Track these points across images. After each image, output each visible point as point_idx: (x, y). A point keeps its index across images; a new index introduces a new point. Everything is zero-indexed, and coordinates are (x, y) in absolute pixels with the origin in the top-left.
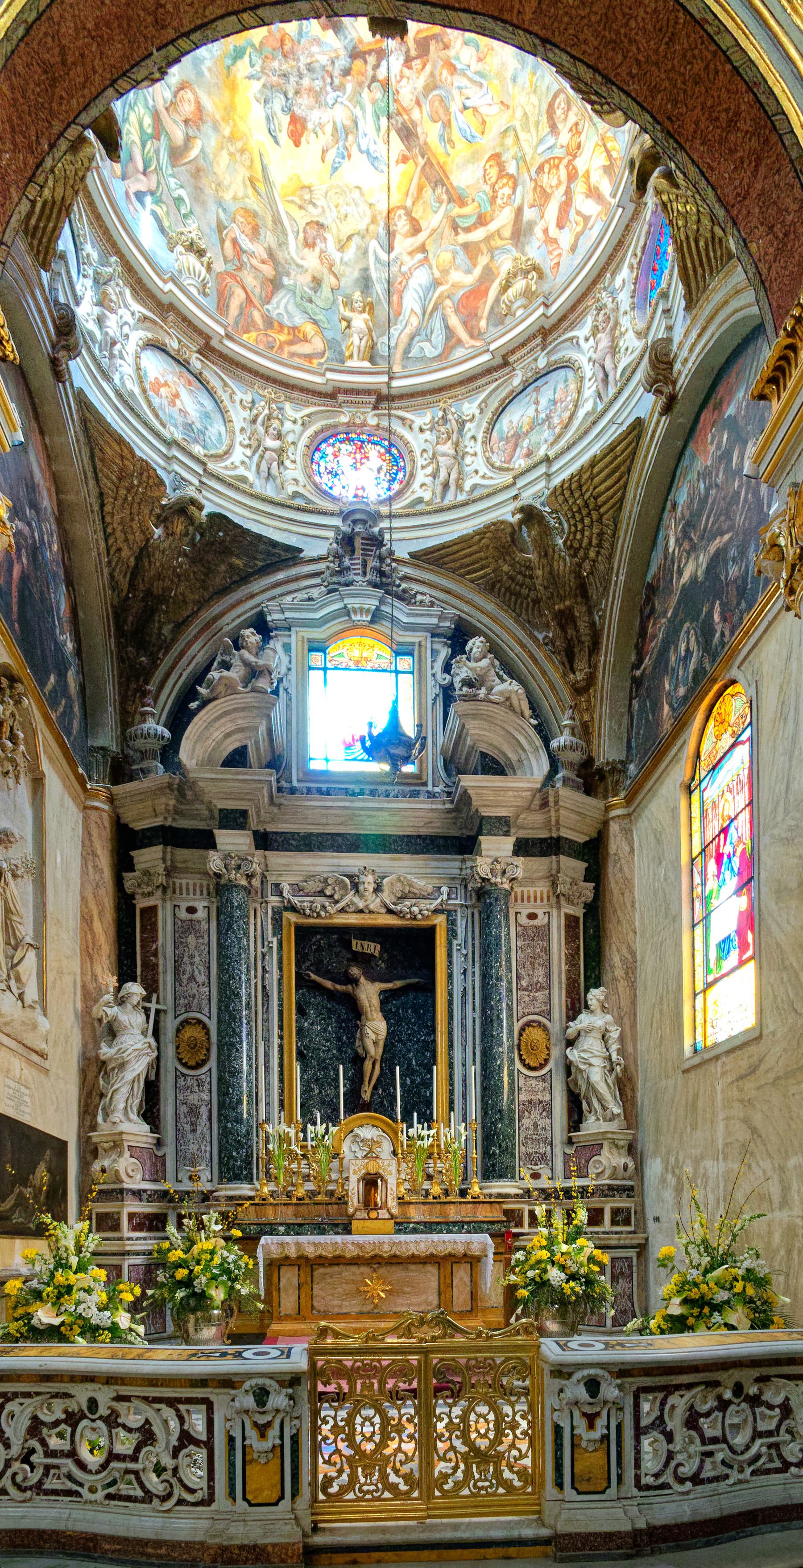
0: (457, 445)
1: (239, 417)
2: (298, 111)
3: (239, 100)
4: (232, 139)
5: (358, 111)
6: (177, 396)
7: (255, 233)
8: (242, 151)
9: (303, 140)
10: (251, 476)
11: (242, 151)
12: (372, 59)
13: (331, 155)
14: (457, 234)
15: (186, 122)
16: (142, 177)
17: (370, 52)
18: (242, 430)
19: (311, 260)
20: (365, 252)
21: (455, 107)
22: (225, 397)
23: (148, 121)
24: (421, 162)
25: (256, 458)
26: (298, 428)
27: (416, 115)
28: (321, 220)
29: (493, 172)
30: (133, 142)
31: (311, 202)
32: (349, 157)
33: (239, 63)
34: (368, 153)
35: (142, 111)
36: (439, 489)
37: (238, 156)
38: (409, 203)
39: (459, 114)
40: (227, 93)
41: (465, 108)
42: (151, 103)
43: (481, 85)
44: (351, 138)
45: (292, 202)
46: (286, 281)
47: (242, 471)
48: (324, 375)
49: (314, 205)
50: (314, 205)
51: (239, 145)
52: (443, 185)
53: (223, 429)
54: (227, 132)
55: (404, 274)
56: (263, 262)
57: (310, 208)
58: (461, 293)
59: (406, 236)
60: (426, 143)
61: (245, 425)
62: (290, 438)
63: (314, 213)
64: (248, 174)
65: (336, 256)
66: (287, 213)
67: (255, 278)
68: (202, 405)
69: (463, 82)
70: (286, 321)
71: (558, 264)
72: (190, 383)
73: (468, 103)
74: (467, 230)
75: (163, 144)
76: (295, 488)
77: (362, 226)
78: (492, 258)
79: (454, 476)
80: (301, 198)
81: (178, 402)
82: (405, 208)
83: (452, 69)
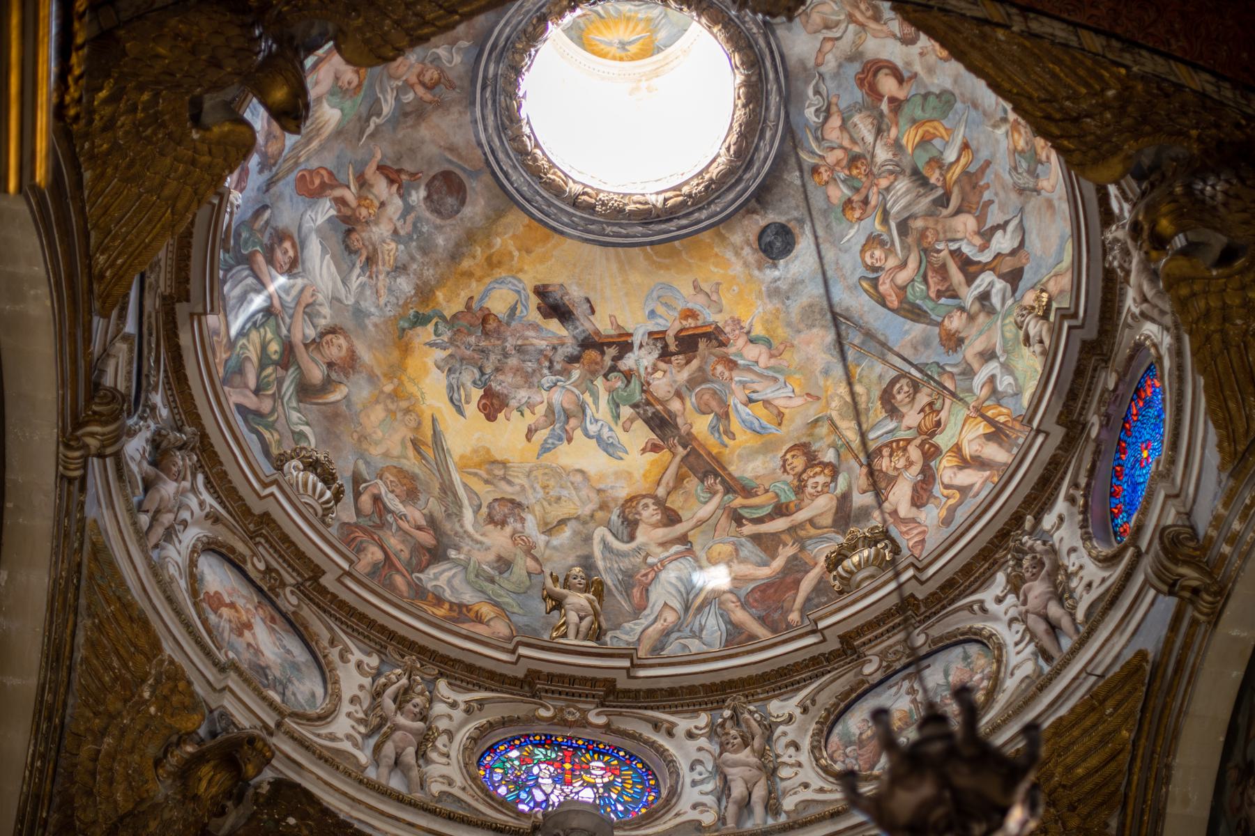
0: (762, 754)
1: (352, 681)
2: (496, 387)
3: (412, 363)
4: (395, 396)
5: (587, 398)
6: (249, 626)
7: (411, 495)
8: (407, 411)
9: (501, 416)
10: (363, 757)
11: (407, 411)
12: (612, 352)
13: (543, 434)
14: (740, 524)
15: (330, 365)
16: (252, 395)
17: (610, 345)
18: (354, 700)
19: (499, 540)
20: (588, 539)
21: (736, 400)
22: (334, 654)
23: (274, 347)
24: (681, 451)
25: (372, 742)
26: (458, 714)
27: (675, 405)
28: (518, 499)
29: (799, 463)
30: (248, 358)
31: (504, 478)
32: (570, 440)
33: (419, 329)
34: (599, 438)
35: (269, 335)
36: (732, 810)
37: (399, 415)
38: (661, 492)
39: (740, 407)
40: (396, 354)
41: (751, 401)
42: (284, 331)
43: (776, 380)
44: (573, 422)
45: (475, 474)
46: (452, 554)
47: (347, 746)
48: (513, 652)
49: (510, 483)
50: (510, 483)
51: (404, 404)
52: (716, 475)
53: (319, 691)
54: (388, 388)
55: (652, 566)
56: (419, 528)
57: (503, 485)
58: (752, 586)
59: (656, 526)
60: (689, 434)
61: (361, 694)
62: (442, 724)
63: (508, 491)
64: (410, 435)
65: (541, 539)
66: (465, 485)
67: (403, 542)
68: (289, 652)
69: (747, 377)
70: (448, 594)
71: (923, 541)
72: (273, 620)
73: (754, 396)
74: (760, 521)
75: (290, 376)
76: (446, 788)
77: (587, 510)
78: (802, 549)
79: (759, 792)
80: (489, 472)
81: (247, 633)
82: (655, 497)
83: (732, 365)
